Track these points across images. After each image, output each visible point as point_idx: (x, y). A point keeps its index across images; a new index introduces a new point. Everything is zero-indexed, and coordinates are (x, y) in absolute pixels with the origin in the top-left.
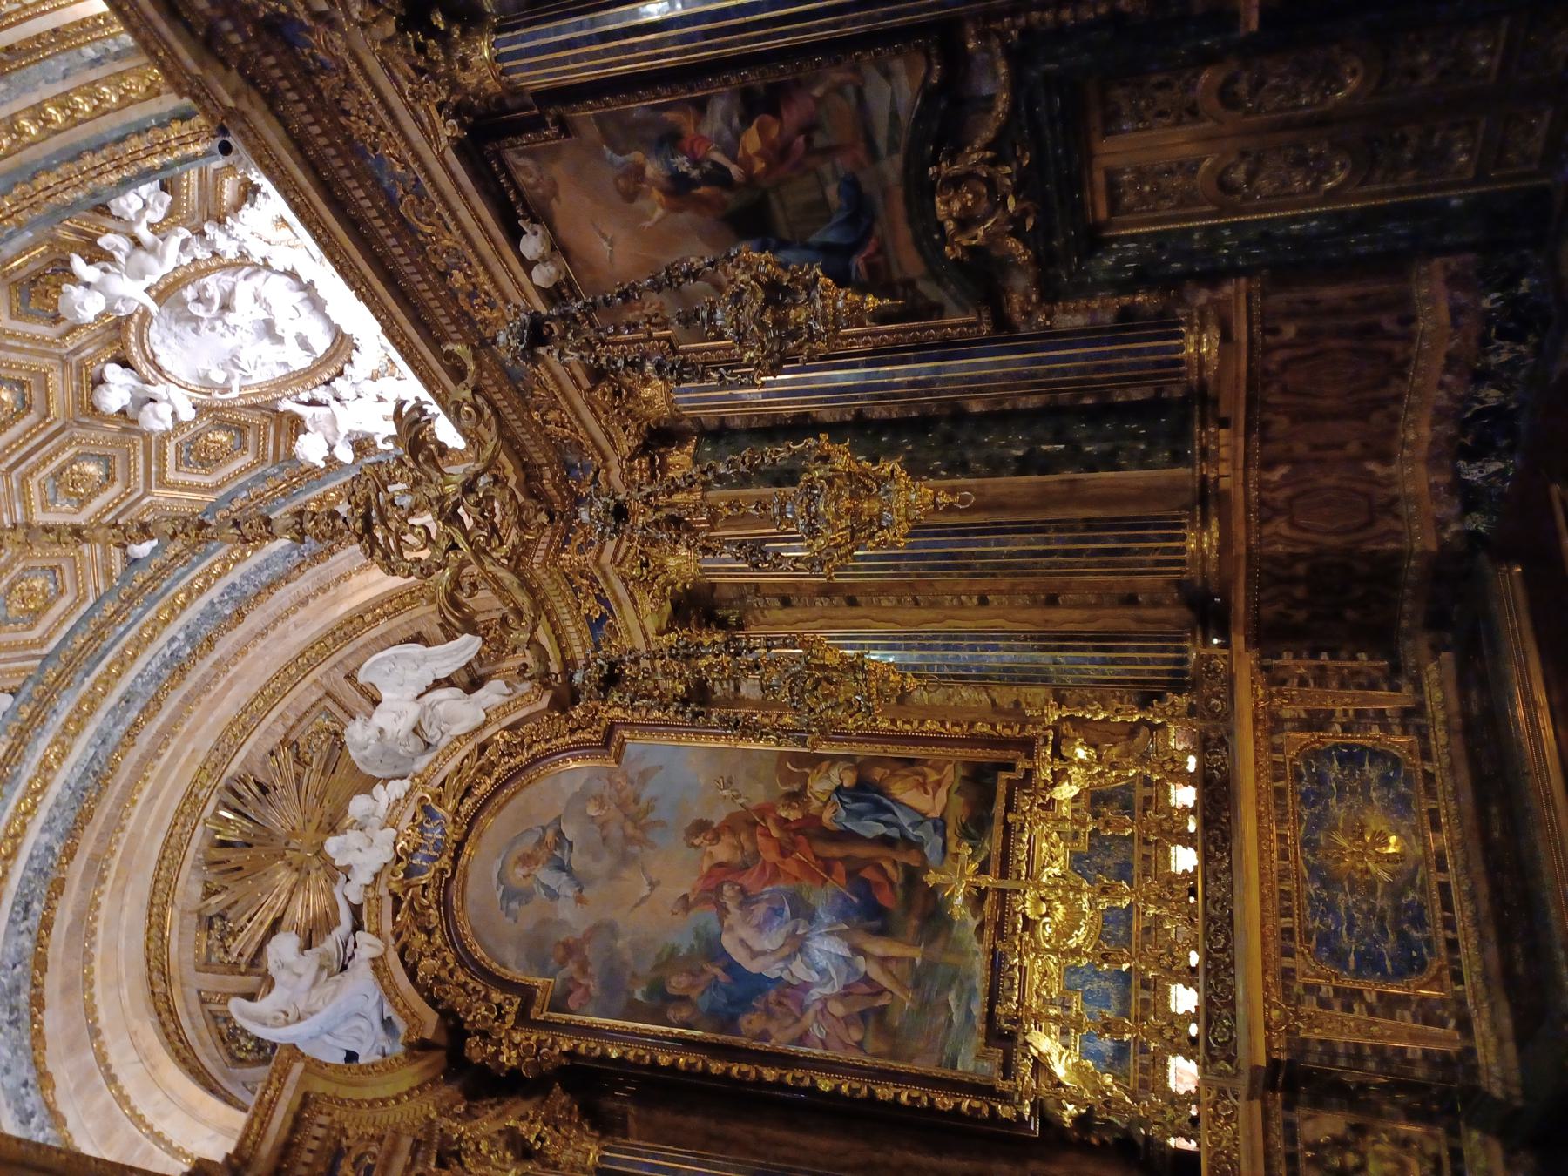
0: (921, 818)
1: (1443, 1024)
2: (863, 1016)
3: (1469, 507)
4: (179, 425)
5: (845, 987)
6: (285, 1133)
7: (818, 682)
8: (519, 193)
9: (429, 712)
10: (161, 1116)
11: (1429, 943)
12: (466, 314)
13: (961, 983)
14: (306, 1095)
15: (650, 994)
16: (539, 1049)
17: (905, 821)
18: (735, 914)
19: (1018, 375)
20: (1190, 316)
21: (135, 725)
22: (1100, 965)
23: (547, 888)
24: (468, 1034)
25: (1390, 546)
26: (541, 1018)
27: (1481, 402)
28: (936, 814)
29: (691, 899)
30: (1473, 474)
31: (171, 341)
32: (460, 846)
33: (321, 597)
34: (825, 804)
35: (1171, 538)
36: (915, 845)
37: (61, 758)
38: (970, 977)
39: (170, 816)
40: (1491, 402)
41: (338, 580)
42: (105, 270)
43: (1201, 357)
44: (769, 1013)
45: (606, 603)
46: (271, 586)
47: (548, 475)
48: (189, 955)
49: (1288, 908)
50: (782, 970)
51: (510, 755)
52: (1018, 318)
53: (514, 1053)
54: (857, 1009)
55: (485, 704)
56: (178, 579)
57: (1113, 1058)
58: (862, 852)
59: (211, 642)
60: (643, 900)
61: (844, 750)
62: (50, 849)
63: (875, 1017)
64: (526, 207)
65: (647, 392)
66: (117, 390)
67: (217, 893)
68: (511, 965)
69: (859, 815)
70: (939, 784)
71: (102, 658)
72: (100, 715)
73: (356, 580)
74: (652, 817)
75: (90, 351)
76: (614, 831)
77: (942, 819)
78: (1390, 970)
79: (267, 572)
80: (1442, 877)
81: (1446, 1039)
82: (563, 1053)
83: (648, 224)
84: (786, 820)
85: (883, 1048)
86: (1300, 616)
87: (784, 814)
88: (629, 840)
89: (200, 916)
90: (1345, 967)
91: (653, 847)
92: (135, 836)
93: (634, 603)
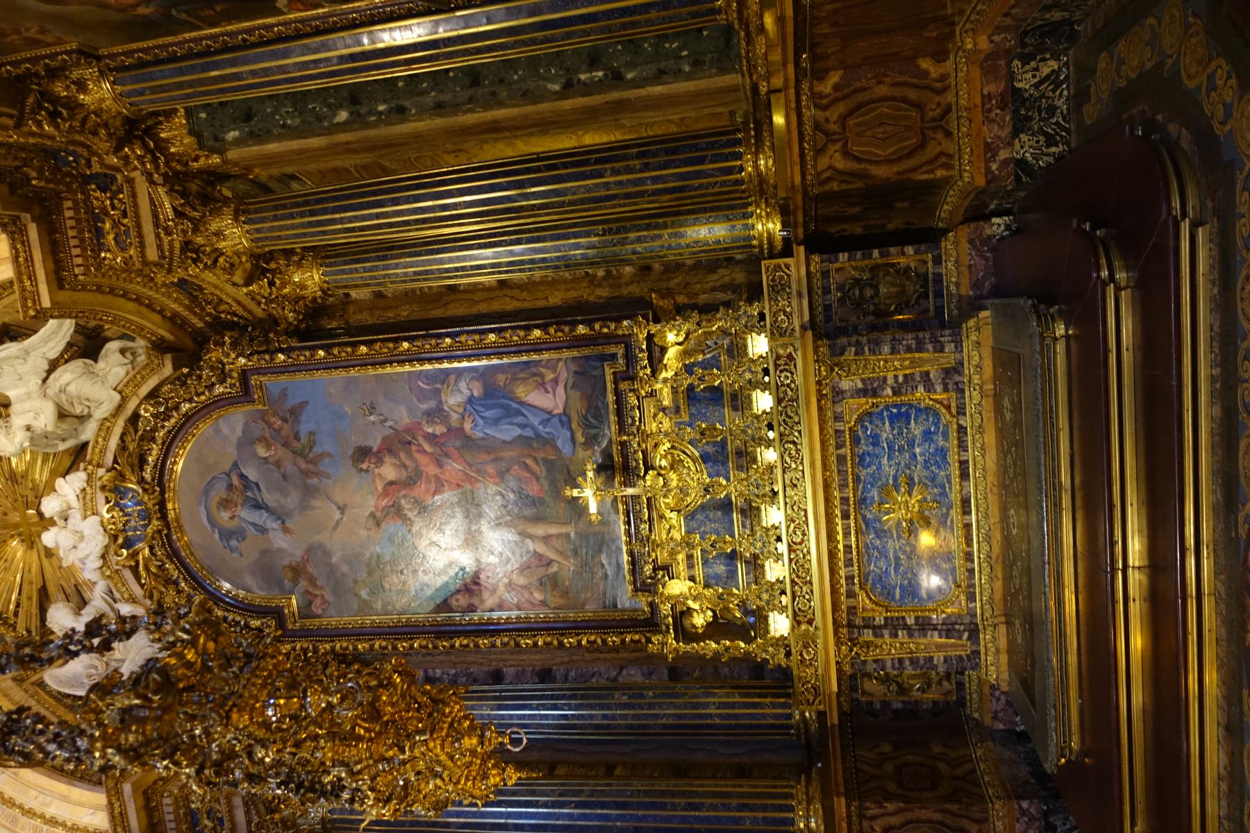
6: (145, 821)
9: (63, 397)
10: (49, 805)
14: (145, 793)
16: (305, 654)
17: (535, 421)
19: (533, 42)
23: (254, 525)
25: (940, 173)
28: (559, 410)
29: (378, 515)
30: (1025, 82)
32: (162, 504)
35: (730, 170)
36: (548, 442)
47: (34, 174)
54: (536, 578)
57: (727, 577)
60: (338, 523)
68: (255, 589)
69: (496, 421)
70: (555, 381)
74: (317, 450)
76: (289, 468)
77: (565, 413)
84: (434, 436)
87: (430, 430)
88: (306, 474)
91: (328, 476)
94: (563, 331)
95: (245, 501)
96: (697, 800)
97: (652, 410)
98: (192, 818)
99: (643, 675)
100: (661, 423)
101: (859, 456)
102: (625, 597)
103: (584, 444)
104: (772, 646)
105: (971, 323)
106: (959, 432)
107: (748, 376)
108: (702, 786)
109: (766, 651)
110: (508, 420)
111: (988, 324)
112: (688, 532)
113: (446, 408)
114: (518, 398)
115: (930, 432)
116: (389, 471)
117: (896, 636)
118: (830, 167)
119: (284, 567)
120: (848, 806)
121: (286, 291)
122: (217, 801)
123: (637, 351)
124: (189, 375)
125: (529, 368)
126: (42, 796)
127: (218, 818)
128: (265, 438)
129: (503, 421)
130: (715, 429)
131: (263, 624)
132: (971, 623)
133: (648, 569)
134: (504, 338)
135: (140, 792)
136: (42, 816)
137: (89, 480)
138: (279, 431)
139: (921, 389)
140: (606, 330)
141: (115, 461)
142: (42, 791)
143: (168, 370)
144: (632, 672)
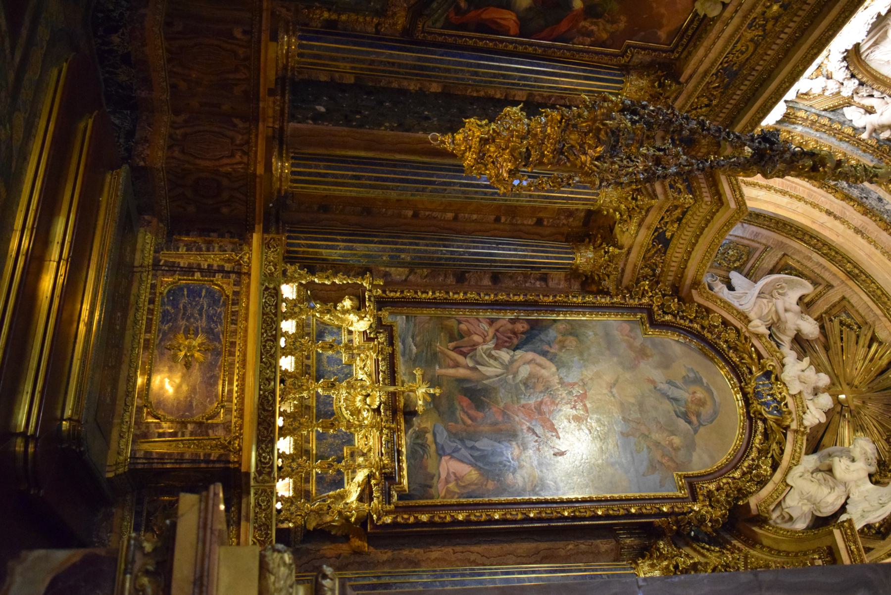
1: (166, 261)
2: (462, 337)
5: (476, 349)
6: (720, 188)
9: (831, 484)
10: (787, 203)
11: (163, 304)
14: (722, 204)
17: (464, 451)
22: (335, 380)
23: (677, 387)
36: (453, 435)
38: (406, 362)
44: (515, 333)
54: (466, 339)
63: (456, 336)
70: (447, 482)
77: (440, 456)
78: (185, 290)
80: (148, 336)
85: (447, 322)
94: (440, 518)
96: (353, 181)
97: (372, 454)
98: (691, 190)
99: (390, 275)
100: (366, 445)
102: (399, 322)
103: (426, 432)
104: (295, 278)
105: (121, 470)
107: (294, 465)
108: (351, 191)
109: (300, 274)
111: (109, 466)
112: (351, 365)
114: (477, 470)
117: (209, 265)
119: (652, 356)
120: (255, 170)
121: (665, 563)
122: (675, 199)
123: (381, 498)
124: (737, 499)
125: (468, 493)
127: (674, 188)
130: (323, 427)
131: (664, 317)
132: (157, 270)
133: (382, 338)
134: (487, 515)
136: (791, 196)
140: (406, 516)
141: (785, 435)
142: (794, 211)
143: (753, 501)
144: (398, 277)
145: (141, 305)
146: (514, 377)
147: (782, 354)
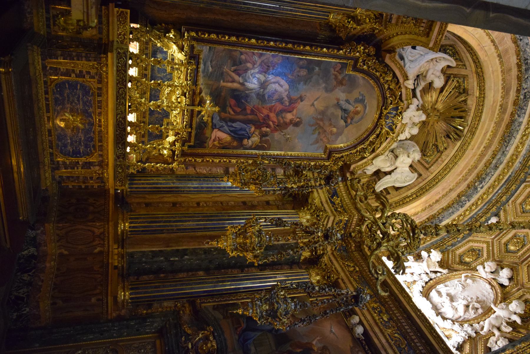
0: (220, 129)
1: (51, 67)
2: (241, 63)
3: (34, 239)
4: (482, 264)
5: (247, 72)
7: (257, 179)
8: (364, 349)
9: (392, 163)
11: (54, 93)
12: (383, 305)
13: (207, 75)
15: (313, 69)
16: (350, 51)
17: (226, 128)
18: (284, 95)
19: (187, 285)
20: (127, 306)
21: (493, 158)
22: (161, 82)
23: (349, 103)
24: (374, 55)
26: (350, 61)
27: (29, 275)
28: (215, 130)
29: (299, 100)
30: (32, 250)
31: (486, 294)
32: (380, 118)
33: (431, 203)
34: (253, 133)
35: (134, 227)
36: (222, 119)
37: (517, 147)
39: (480, 127)
40: (26, 275)
41: (425, 209)
42: (510, 319)
43: (124, 291)
45: (331, 202)
46: (449, 207)
47: (353, 248)
48: (470, 80)
49: (98, 103)
50: (268, 77)
51: (364, 148)
52: (187, 305)
53: (359, 49)
55: (373, 166)
56: (481, 209)
57: (157, 52)
58: (241, 117)
59: (469, 187)
61: (247, 151)
62: (519, 116)
64: (362, 344)
65: (318, 278)
66: (504, 275)
67: (462, 101)
68: (361, 78)
69: (241, 129)
70: (214, 141)
71: (506, 181)
72: (505, 161)
73: (419, 209)
74: (313, 128)
75: (514, 290)
76: (327, 123)
77: (213, 129)
78: (67, 85)
79: (450, 211)
80: (49, 115)
81: (51, 63)
82: (342, 50)
83: (318, 338)
84: (267, 127)
85: (234, 53)
86: (91, 200)
87: (268, 129)
89: (468, 93)
90: (81, 84)
92: (491, 121)
93: (321, 202)
95: (349, 113)
101: (93, 141)
106: (52, 147)
110: (236, 129)
112: (171, 74)
113: (259, 136)
115: (64, 147)
116: (289, 116)
117: (80, 71)
118: (99, 229)
119: (345, 85)
126: (474, 34)
128: (331, 134)
129: (239, 129)
135: (429, 38)
137: (398, 135)
138: (325, 136)
139: (68, 163)
145: (40, 98)
146: (264, 91)
147: (411, 102)
